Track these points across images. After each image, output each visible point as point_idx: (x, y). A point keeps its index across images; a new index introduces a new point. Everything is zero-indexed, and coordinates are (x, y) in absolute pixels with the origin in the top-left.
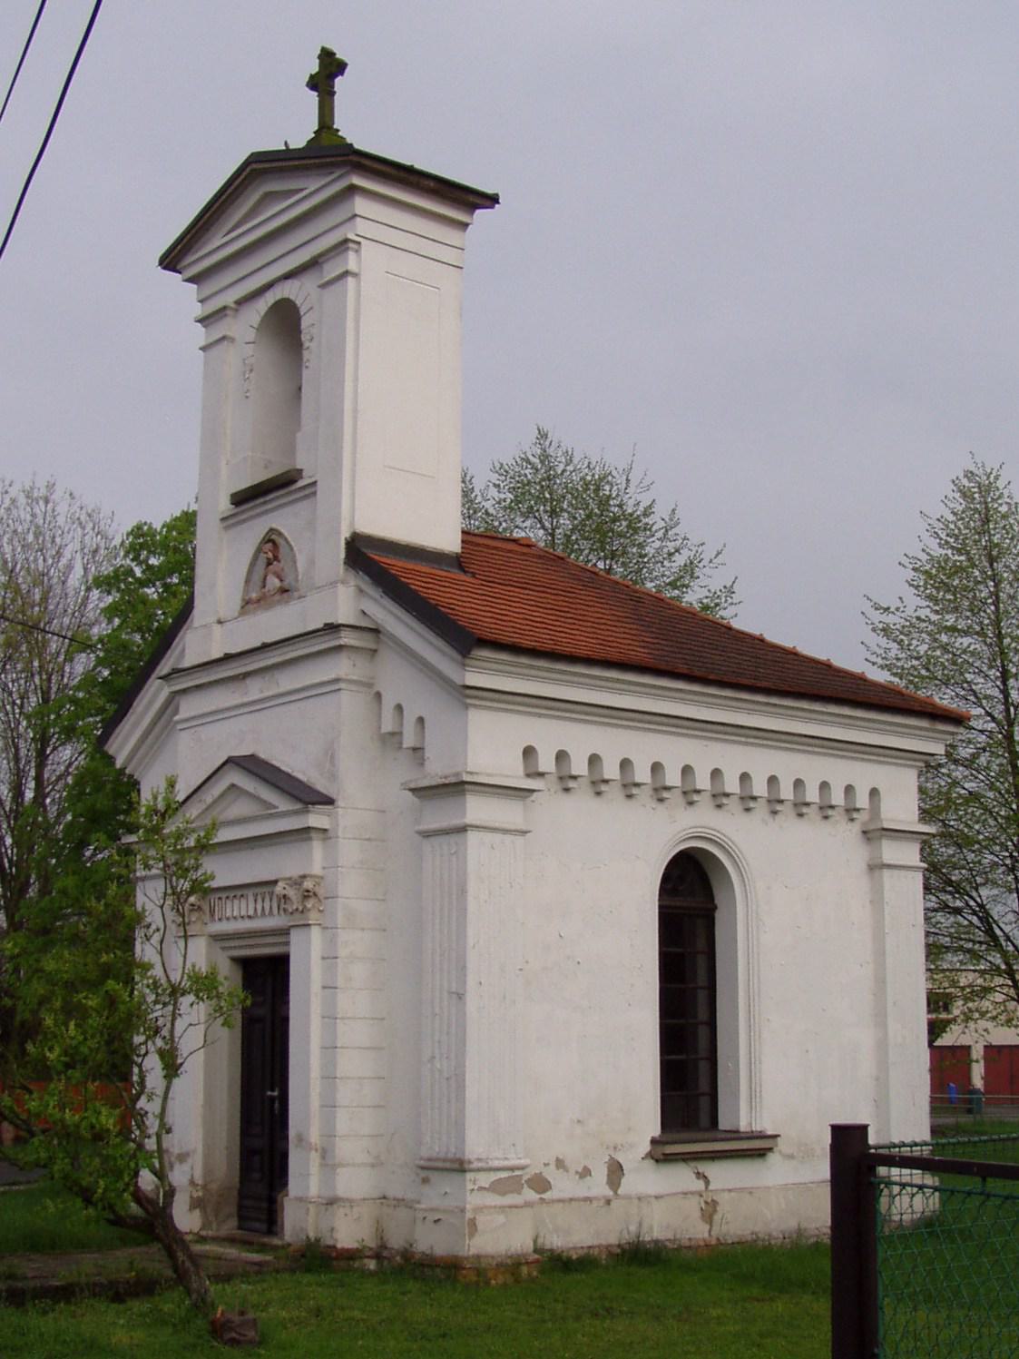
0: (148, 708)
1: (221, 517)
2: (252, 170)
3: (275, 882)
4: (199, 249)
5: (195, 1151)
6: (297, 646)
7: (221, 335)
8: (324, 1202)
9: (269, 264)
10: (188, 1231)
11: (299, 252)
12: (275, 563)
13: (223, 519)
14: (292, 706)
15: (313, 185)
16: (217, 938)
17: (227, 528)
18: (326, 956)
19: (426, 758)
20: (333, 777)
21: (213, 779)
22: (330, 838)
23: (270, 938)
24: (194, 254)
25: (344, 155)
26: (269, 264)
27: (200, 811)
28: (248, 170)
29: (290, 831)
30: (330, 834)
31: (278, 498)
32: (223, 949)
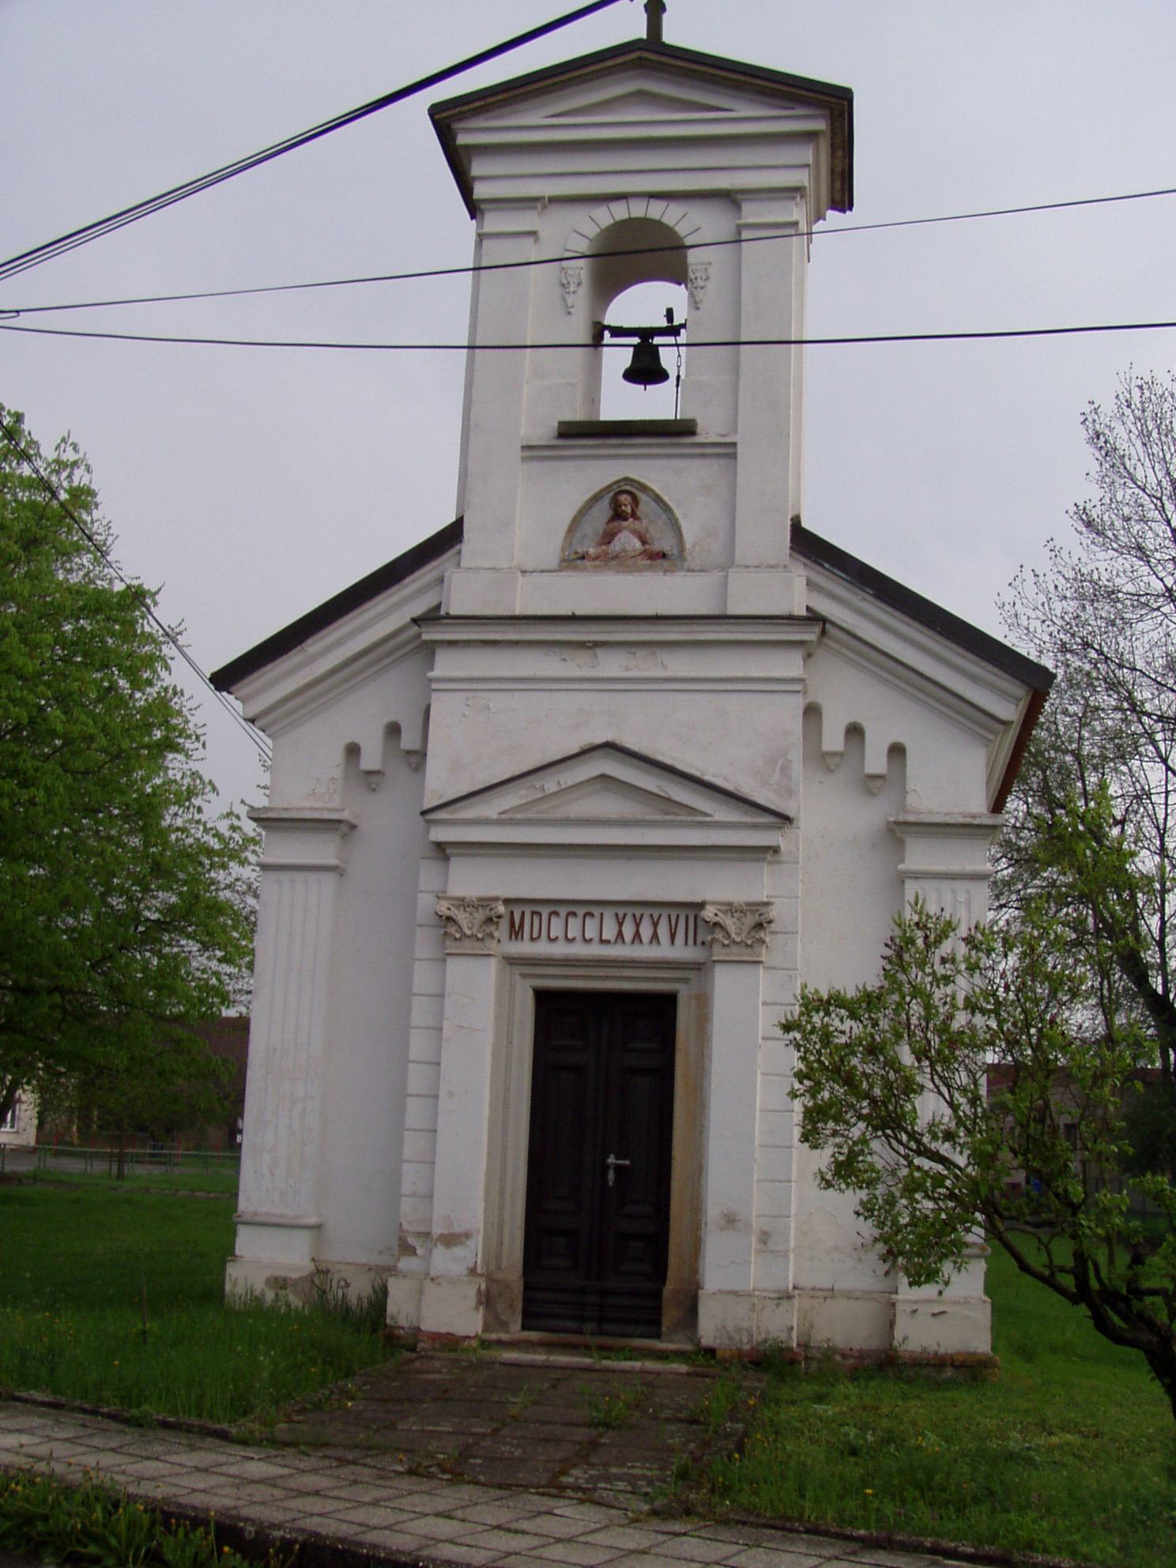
0: (326, 651)
1: (525, 444)
2: (640, 58)
3: (701, 906)
4: (501, 117)
5: (478, 1232)
6: (724, 628)
7: (529, 228)
8: (777, 1295)
9: (622, 172)
10: (473, 1334)
11: (681, 176)
12: (631, 520)
13: (524, 448)
14: (686, 696)
15: (744, 109)
16: (512, 961)
17: (524, 459)
18: (768, 1001)
19: (908, 788)
20: (790, 793)
21: (569, 763)
22: (780, 862)
23: (642, 971)
24: (486, 119)
25: (838, 98)
26: (622, 172)
27: (534, 798)
28: (634, 56)
29: (728, 847)
30: (784, 856)
31: (649, 446)
32: (524, 976)
